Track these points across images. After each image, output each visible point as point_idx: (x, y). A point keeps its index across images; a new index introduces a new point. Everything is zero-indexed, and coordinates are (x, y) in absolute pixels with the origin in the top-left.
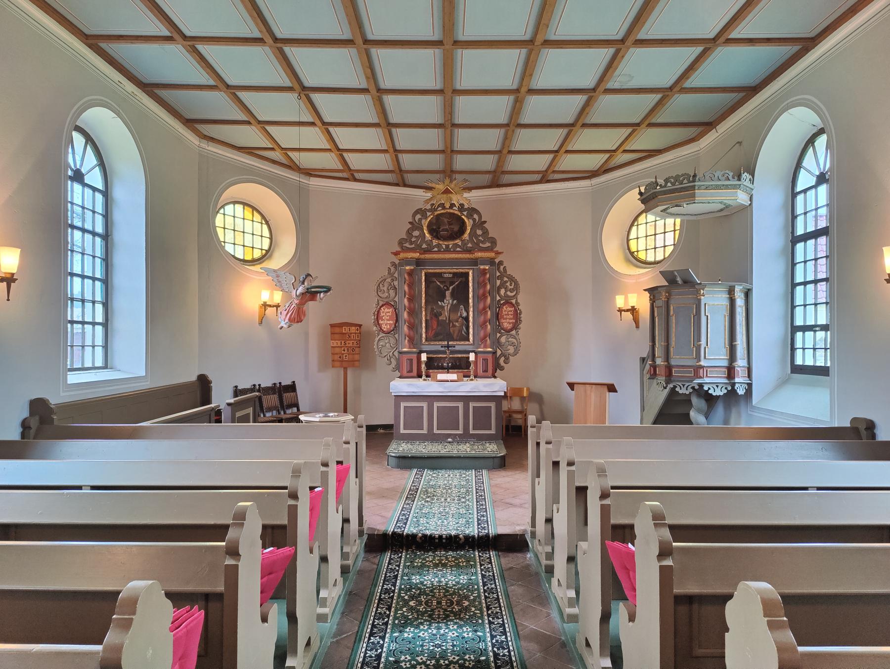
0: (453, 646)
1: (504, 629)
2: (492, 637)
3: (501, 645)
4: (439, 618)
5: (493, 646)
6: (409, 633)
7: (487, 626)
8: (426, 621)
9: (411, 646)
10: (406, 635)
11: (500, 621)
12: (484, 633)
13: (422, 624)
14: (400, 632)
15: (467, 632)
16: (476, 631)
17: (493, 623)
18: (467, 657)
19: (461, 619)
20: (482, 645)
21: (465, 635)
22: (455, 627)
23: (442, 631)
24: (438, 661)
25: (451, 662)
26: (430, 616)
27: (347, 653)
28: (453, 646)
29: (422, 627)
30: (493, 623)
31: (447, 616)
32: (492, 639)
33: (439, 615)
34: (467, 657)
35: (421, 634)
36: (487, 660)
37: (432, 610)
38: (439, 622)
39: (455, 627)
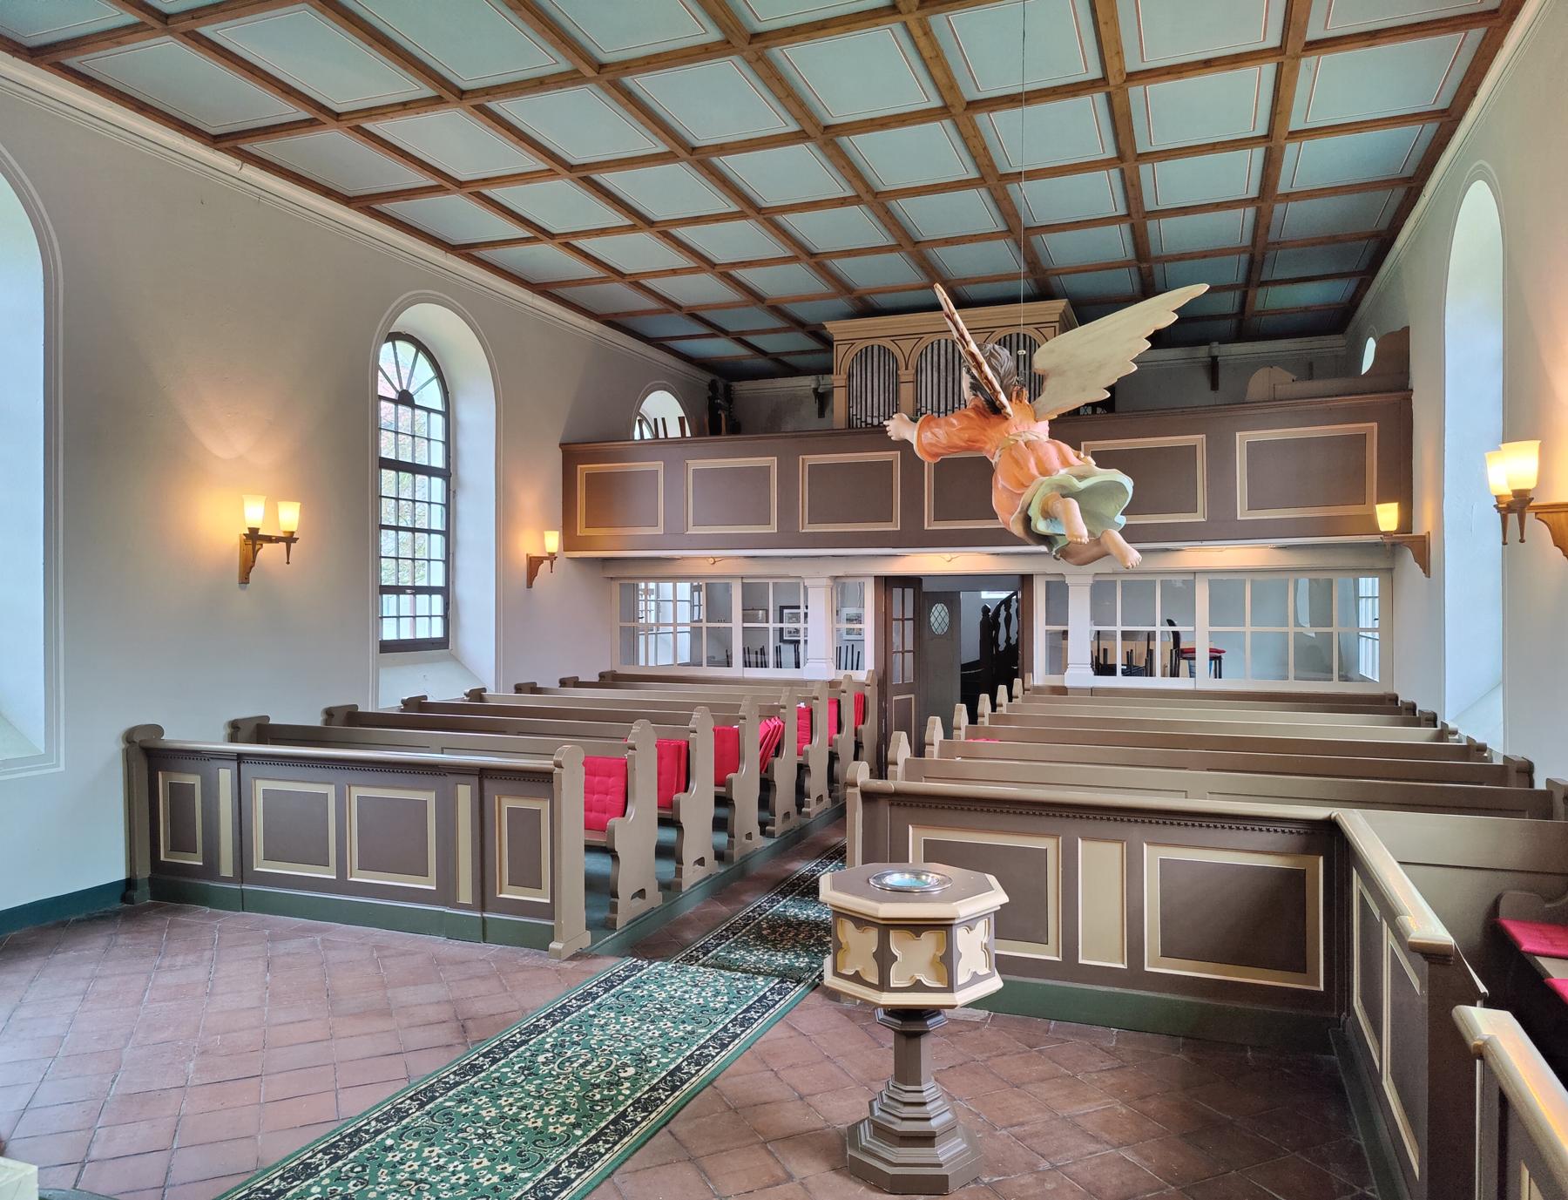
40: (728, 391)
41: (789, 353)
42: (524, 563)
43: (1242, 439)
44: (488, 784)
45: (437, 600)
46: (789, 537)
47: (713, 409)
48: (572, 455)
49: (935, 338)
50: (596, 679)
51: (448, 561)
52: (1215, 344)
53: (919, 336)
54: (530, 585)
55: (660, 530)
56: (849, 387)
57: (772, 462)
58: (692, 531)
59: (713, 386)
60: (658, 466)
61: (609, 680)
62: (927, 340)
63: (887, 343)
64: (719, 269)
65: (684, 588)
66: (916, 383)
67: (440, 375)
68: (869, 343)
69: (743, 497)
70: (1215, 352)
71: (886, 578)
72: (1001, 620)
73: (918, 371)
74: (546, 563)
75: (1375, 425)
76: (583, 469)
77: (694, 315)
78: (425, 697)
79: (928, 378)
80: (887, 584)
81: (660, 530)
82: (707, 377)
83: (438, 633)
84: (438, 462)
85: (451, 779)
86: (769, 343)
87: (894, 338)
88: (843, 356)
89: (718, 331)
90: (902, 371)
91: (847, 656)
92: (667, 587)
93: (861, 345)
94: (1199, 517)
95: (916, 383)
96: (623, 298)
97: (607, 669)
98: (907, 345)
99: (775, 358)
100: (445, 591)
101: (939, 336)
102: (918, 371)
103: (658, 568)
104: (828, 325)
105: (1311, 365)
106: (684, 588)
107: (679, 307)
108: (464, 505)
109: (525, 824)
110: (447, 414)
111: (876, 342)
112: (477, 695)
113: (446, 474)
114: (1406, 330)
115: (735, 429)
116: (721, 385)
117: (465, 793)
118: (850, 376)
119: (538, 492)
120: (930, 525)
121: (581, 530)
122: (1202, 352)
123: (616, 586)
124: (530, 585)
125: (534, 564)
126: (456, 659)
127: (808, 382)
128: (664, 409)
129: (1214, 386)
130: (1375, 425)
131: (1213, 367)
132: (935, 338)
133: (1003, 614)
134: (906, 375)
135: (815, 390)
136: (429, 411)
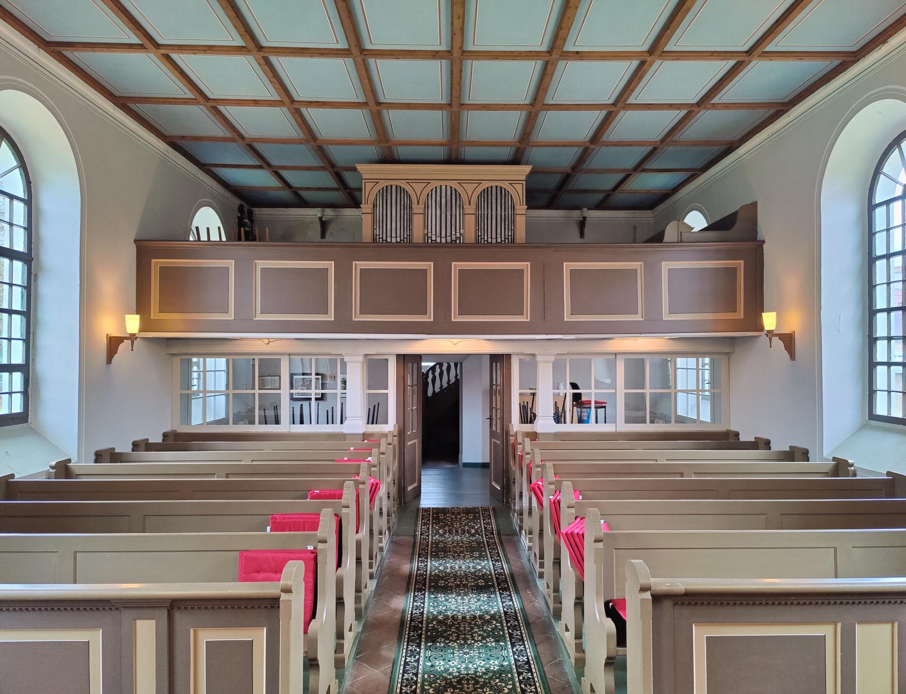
0: (453, 653)
1: (404, 667)
2: (418, 661)
3: (412, 654)
4: (468, 680)
5: (419, 653)
6: (494, 664)
7: (420, 671)
8: (481, 677)
9: (489, 653)
10: (496, 662)
11: (406, 676)
12: (424, 664)
13: (484, 674)
14: (502, 666)
15: (440, 665)
16: (432, 666)
17: (413, 674)
18: (442, 645)
19: (445, 679)
20: (429, 653)
21: (442, 663)
22: (451, 670)
23: (464, 666)
24: (465, 642)
25: (455, 641)
26: (477, 682)
27: (541, 648)
28: (453, 653)
29: (483, 670)
30: (413, 674)
31: (459, 682)
32: (419, 659)
33: (468, 684)
34: (442, 645)
35: (483, 663)
36: (426, 643)
37: (476, 689)
38: (467, 674)
39: (451, 670)
40: (250, 213)
41: (309, 189)
42: (104, 342)
43: (666, 266)
44: (178, 616)
45: (18, 376)
46: (343, 324)
47: (241, 224)
48: (145, 251)
49: (438, 184)
50: (159, 440)
51: (29, 340)
52: (585, 209)
53: (428, 182)
54: (109, 360)
55: (231, 316)
56: (373, 214)
57: (330, 265)
58: (260, 317)
59: (241, 208)
60: (231, 264)
61: (176, 441)
62: (433, 184)
63: (403, 184)
64: (296, 105)
65: (222, 362)
66: (425, 215)
67: (23, 165)
68: (389, 183)
69: (306, 293)
70: (585, 215)
71: (404, 355)
72: (430, 380)
73: (426, 207)
74: (127, 343)
75: (742, 262)
76: (156, 263)
77: (251, 147)
78: (12, 476)
79: (433, 212)
80: (403, 359)
81: (231, 316)
82: (237, 202)
83: (17, 408)
84: (20, 246)
85: (126, 615)
86: (293, 178)
87: (409, 181)
88: (369, 192)
89: (264, 163)
90: (415, 205)
91: (374, 415)
92: (210, 361)
93: (383, 184)
94: (638, 318)
95: (425, 215)
96: (199, 121)
97: (168, 429)
98: (418, 187)
99: (295, 191)
100: (25, 369)
101: (444, 184)
102: (426, 207)
103: (209, 348)
104: (360, 167)
105: (635, 227)
106: (222, 362)
107: (242, 137)
108: (47, 288)
109: (231, 664)
110: (29, 202)
111: (394, 183)
112: (63, 468)
113: (28, 258)
114: (754, 205)
115: (254, 240)
116: (246, 207)
117: (146, 632)
118: (375, 206)
119: (116, 280)
120: (456, 318)
121: (155, 314)
122: (576, 214)
123: (177, 361)
124: (109, 360)
125: (114, 344)
126: (36, 433)
127: (316, 213)
128: (208, 222)
129: (582, 235)
130: (742, 262)
131: (582, 224)
132: (438, 184)
133: (431, 376)
134: (417, 208)
135: (320, 218)
136: (12, 197)
